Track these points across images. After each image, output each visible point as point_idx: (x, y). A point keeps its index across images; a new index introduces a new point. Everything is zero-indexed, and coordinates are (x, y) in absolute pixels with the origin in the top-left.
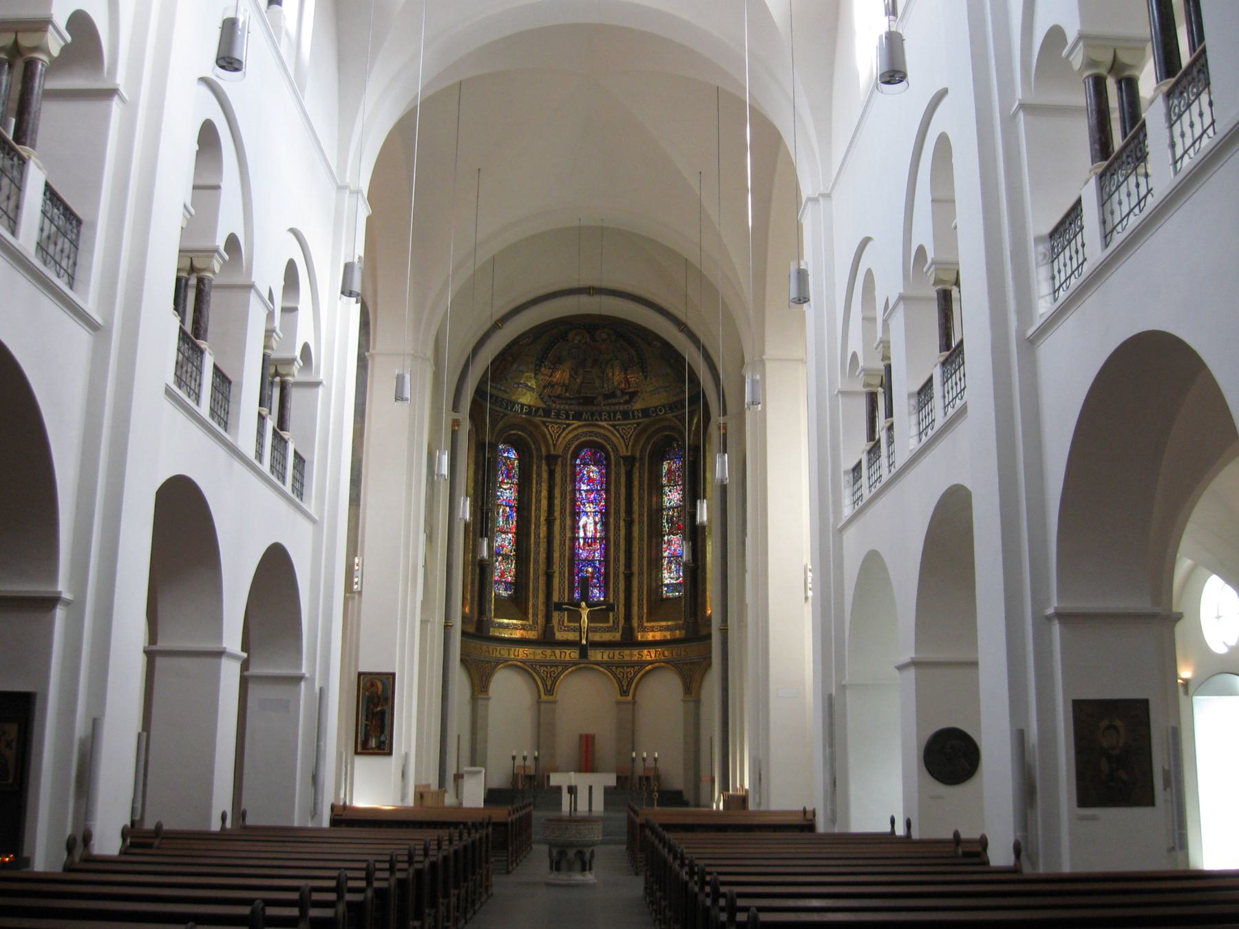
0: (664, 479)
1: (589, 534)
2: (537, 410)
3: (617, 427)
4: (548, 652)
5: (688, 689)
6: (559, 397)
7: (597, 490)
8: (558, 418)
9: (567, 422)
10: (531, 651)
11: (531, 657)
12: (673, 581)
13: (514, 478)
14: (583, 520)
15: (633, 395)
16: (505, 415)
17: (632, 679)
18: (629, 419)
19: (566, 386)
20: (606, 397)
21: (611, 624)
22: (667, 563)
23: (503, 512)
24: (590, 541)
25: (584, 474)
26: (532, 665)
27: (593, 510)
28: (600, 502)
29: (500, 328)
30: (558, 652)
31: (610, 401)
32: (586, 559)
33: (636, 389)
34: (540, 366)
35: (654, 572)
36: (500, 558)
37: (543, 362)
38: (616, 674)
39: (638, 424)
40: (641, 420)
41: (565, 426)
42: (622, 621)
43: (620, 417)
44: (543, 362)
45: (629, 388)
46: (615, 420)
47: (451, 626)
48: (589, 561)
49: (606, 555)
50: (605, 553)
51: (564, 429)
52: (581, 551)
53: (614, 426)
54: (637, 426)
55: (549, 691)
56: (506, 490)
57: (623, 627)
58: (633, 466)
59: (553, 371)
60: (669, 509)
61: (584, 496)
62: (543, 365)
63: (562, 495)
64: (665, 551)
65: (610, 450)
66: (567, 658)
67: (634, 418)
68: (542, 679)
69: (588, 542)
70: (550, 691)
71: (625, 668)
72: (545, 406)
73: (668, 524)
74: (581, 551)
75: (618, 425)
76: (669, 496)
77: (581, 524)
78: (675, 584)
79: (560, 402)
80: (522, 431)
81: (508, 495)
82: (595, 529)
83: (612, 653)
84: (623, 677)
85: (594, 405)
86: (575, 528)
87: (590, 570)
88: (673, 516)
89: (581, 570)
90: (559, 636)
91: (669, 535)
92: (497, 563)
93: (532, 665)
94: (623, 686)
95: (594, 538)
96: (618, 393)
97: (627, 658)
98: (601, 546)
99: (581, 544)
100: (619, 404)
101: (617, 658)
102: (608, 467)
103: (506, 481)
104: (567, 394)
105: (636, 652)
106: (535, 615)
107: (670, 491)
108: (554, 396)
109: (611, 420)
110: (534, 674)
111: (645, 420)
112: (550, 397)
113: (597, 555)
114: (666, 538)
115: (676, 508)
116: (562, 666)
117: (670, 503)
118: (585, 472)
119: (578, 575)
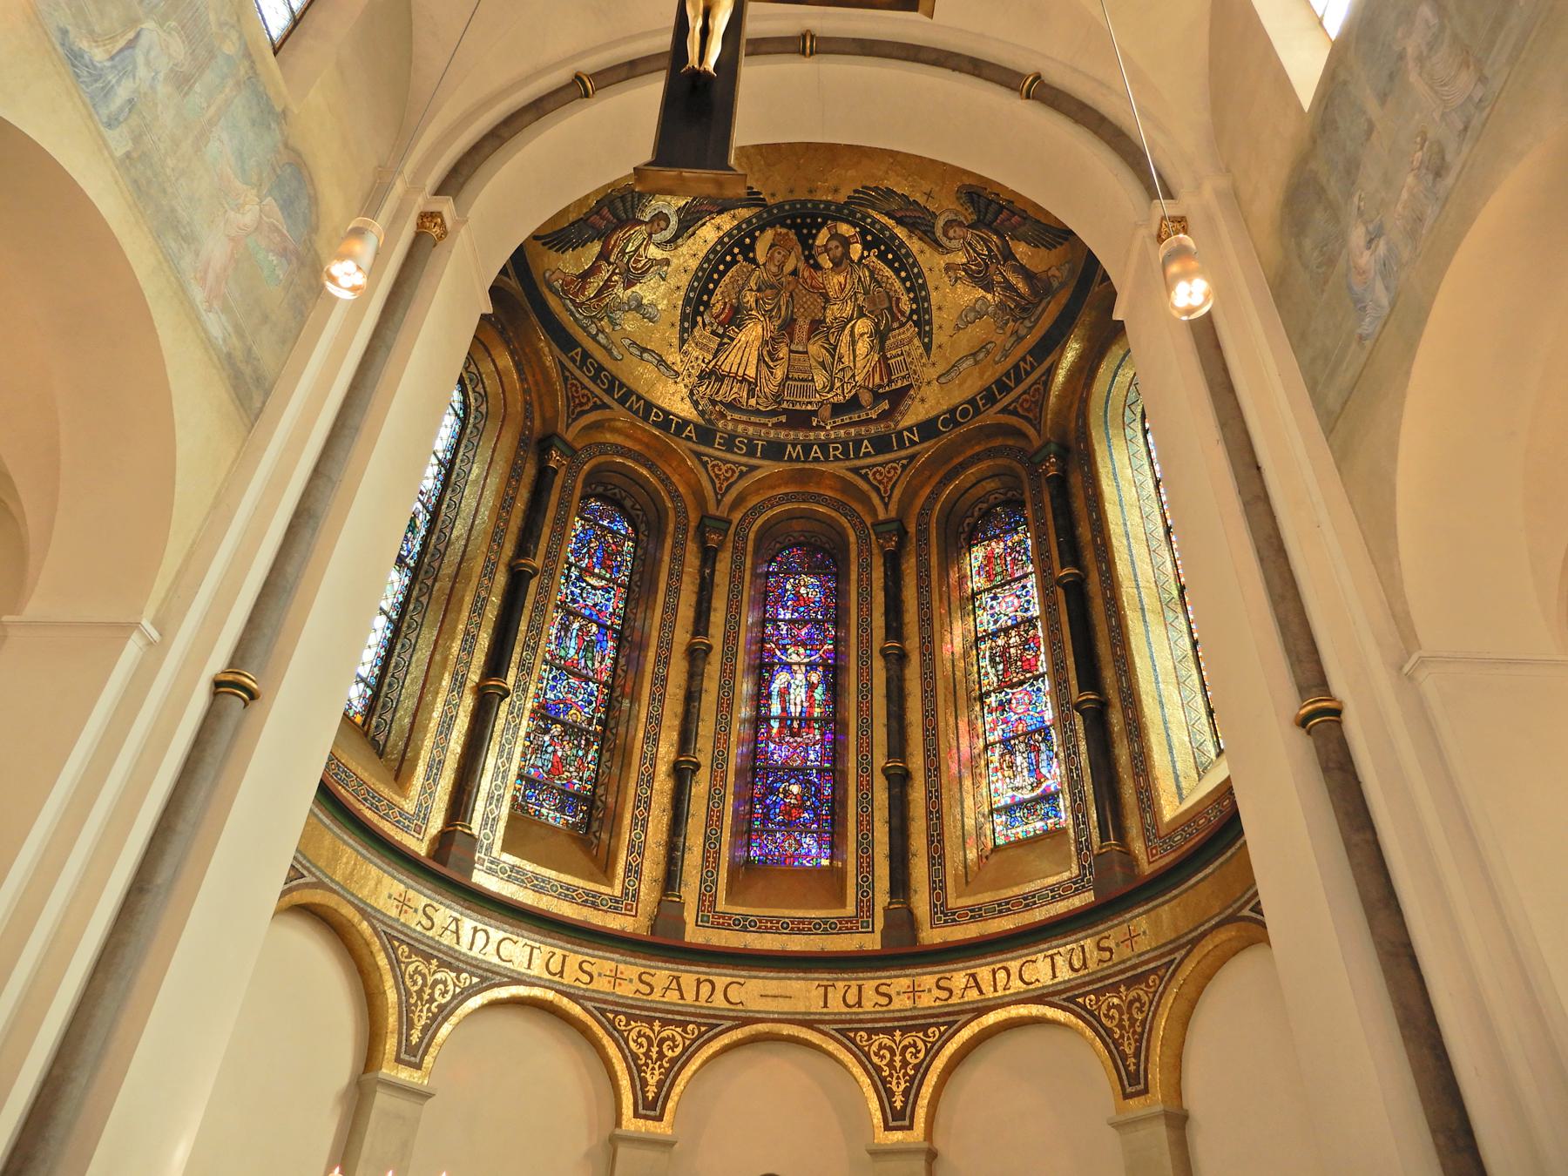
0: (976, 578)
1: (795, 710)
2: (686, 422)
3: (863, 471)
4: (662, 975)
5: (1134, 1078)
6: (732, 406)
7: (817, 621)
8: (730, 450)
9: (754, 462)
10: (608, 966)
11: (602, 985)
12: (1027, 795)
13: (618, 572)
14: (781, 679)
15: (898, 397)
16: (605, 406)
17: (922, 1069)
18: (890, 450)
19: (750, 383)
20: (837, 409)
21: (850, 910)
22: (1002, 755)
23: (580, 629)
24: (796, 725)
25: (787, 591)
26: (603, 1012)
27: (806, 660)
28: (823, 643)
29: (587, 95)
30: (688, 980)
31: (846, 419)
32: (784, 766)
33: (906, 383)
34: (695, 324)
35: (967, 783)
36: (557, 729)
37: (702, 314)
38: (867, 1055)
39: (912, 458)
40: (917, 448)
41: (744, 469)
42: (882, 898)
43: (870, 449)
44: (702, 314)
45: (890, 381)
46: (857, 457)
47: (253, 695)
48: (793, 769)
49: (835, 753)
50: (834, 750)
51: (742, 475)
52: (772, 746)
53: (856, 470)
54: (909, 463)
55: (651, 1105)
56: (594, 588)
57: (886, 910)
58: (901, 544)
59: (721, 344)
60: (995, 634)
61: (784, 632)
62: (699, 319)
63: (729, 607)
64: (993, 730)
65: (847, 525)
66: (719, 1001)
67: (901, 446)
68: (632, 1060)
69: (791, 728)
70: (650, 1107)
71: (898, 1033)
72: (701, 421)
73: (993, 663)
74: (772, 746)
75: (868, 467)
76: (992, 607)
77: (776, 687)
78: (1030, 801)
79: (736, 416)
80: (649, 469)
81: (598, 599)
82: (810, 698)
83: (854, 990)
84: (891, 1064)
85: (813, 428)
86: (761, 697)
87: (795, 789)
88: (1007, 647)
89: (772, 790)
90: (694, 935)
91: (999, 689)
92: (547, 738)
93: (603, 1012)
94: (890, 1093)
95: (806, 720)
96: (866, 398)
97: (901, 1003)
98: (823, 734)
99: (774, 731)
100: (869, 421)
101: (870, 1001)
102: (841, 576)
103: (596, 571)
104: (753, 402)
105: (928, 981)
106: (634, 871)
107: (994, 598)
108: (721, 402)
109: (848, 458)
110: (607, 1041)
111: (926, 445)
112: (714, 403)
113: (812, 757)
114: (992, 700)
115: (1012, 627)
116: (699, 1025)
117: (996, 622)
118: (789, 587)
119: (762, 801)
